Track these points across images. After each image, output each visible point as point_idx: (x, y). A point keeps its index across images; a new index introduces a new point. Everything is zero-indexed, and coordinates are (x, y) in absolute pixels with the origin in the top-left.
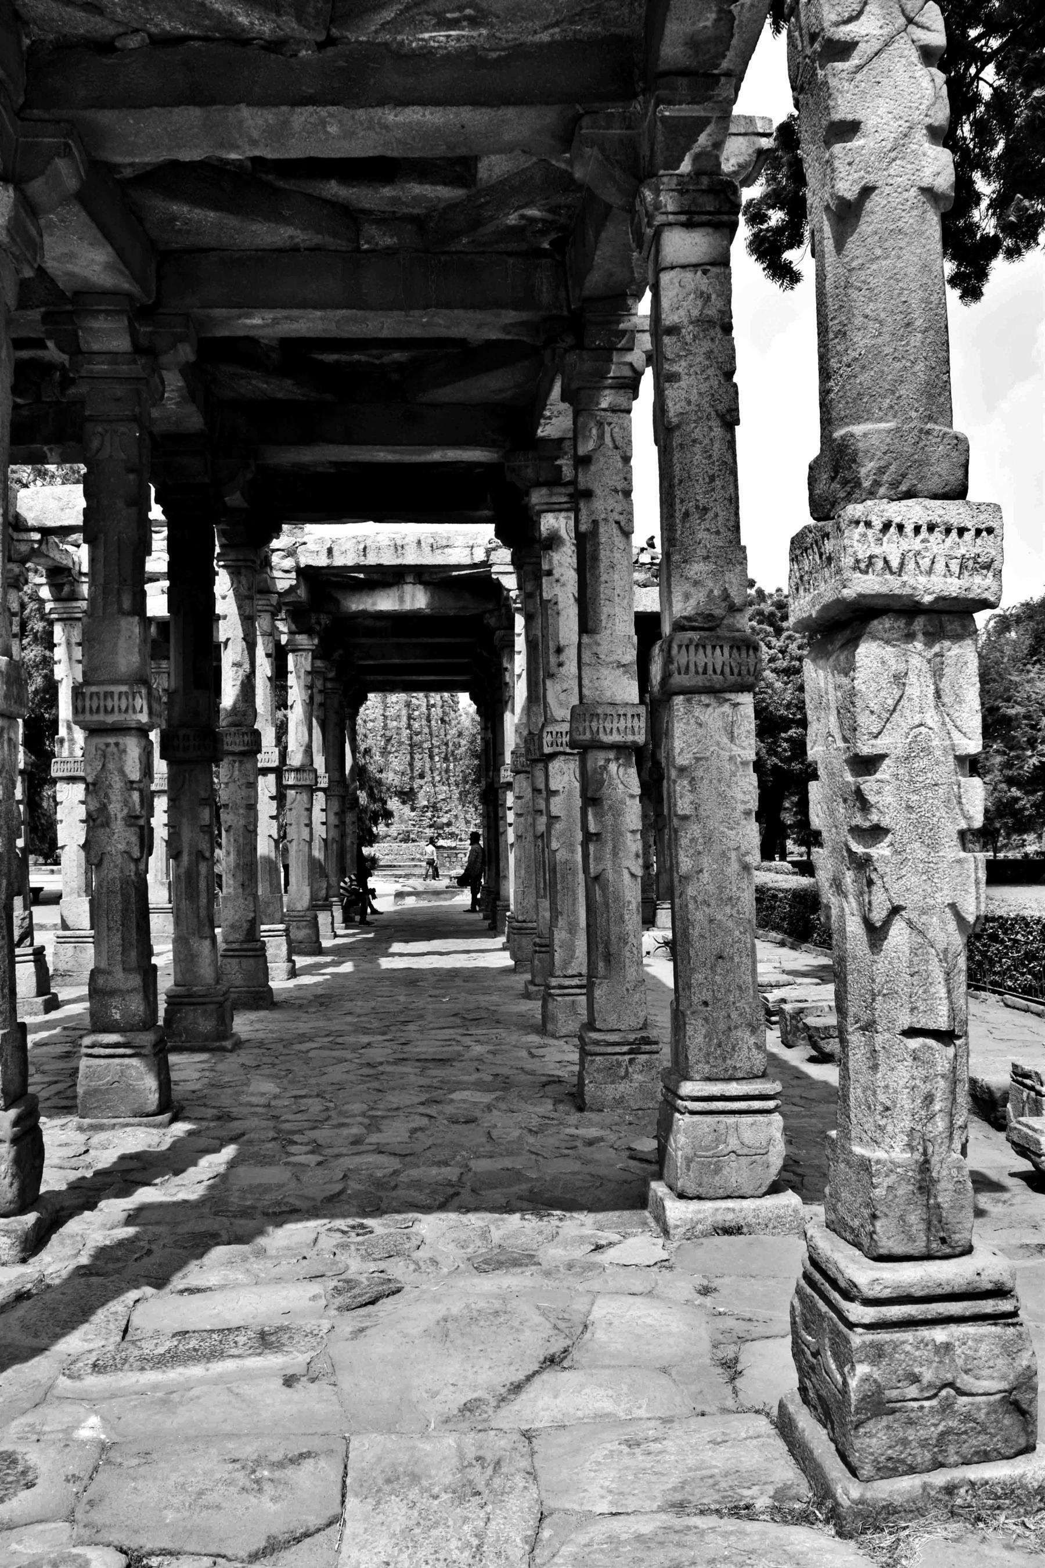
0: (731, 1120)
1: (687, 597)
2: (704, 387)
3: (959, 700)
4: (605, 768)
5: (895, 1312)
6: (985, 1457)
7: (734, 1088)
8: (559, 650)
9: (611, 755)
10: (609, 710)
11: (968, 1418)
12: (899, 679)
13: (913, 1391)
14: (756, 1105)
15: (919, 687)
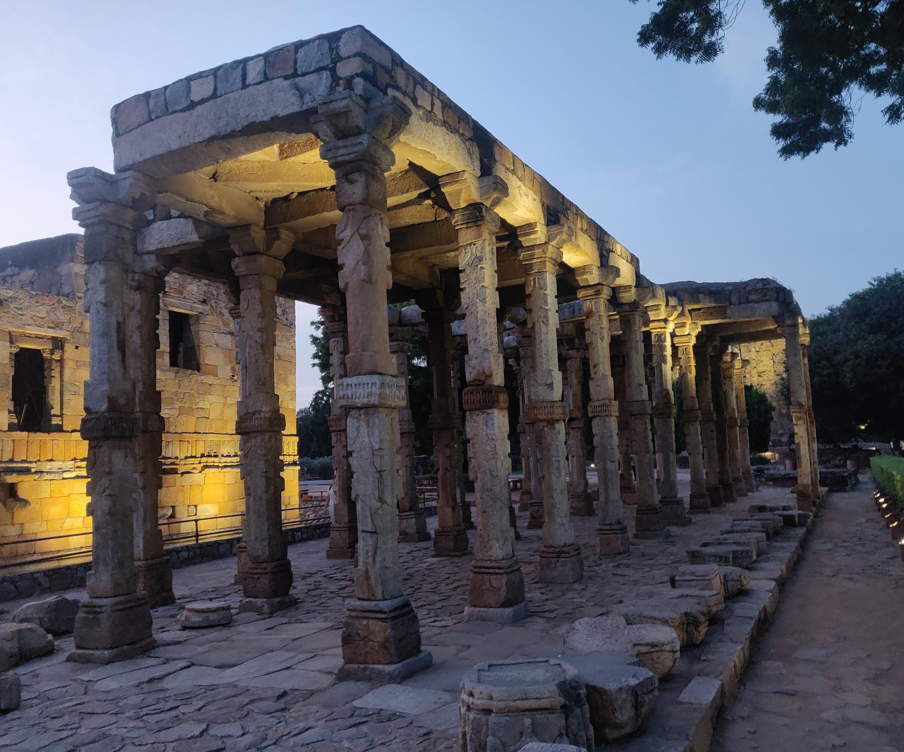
0: (486, 576)
1: (470, 373)
2: (474, 291)
3: (373, 433)
4: (543, 430)
5: (354, 614)
6: (379, 663)
7: (488, 564)
8: (595, 366)
9: (545, 424)
10: (541, 405)
11: (372, 648)
12: (358, 428)
13: (357, 638)
14: (497, 571)
15: (364, 430)
